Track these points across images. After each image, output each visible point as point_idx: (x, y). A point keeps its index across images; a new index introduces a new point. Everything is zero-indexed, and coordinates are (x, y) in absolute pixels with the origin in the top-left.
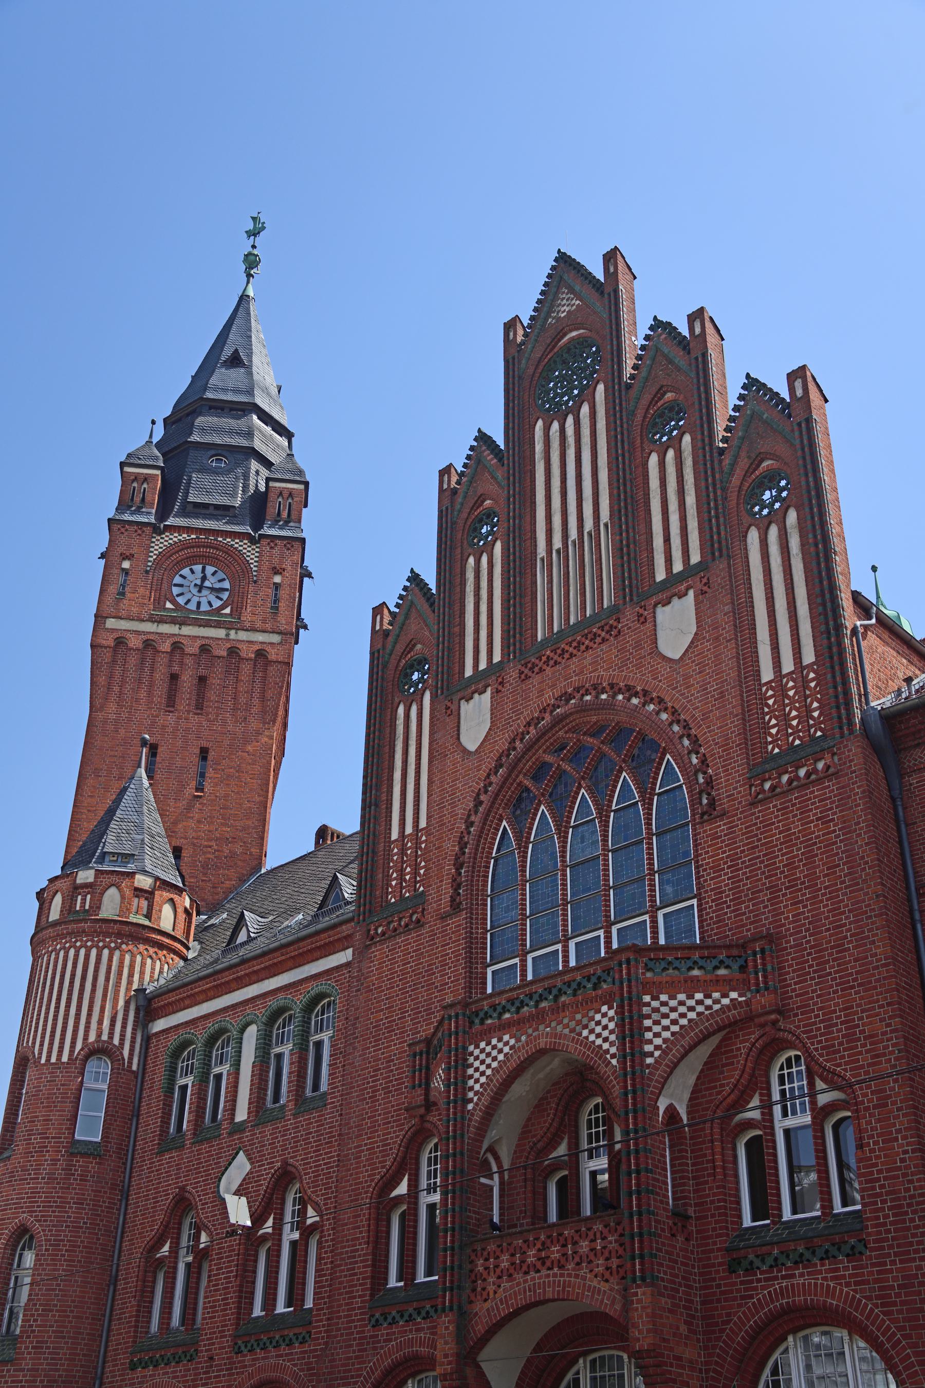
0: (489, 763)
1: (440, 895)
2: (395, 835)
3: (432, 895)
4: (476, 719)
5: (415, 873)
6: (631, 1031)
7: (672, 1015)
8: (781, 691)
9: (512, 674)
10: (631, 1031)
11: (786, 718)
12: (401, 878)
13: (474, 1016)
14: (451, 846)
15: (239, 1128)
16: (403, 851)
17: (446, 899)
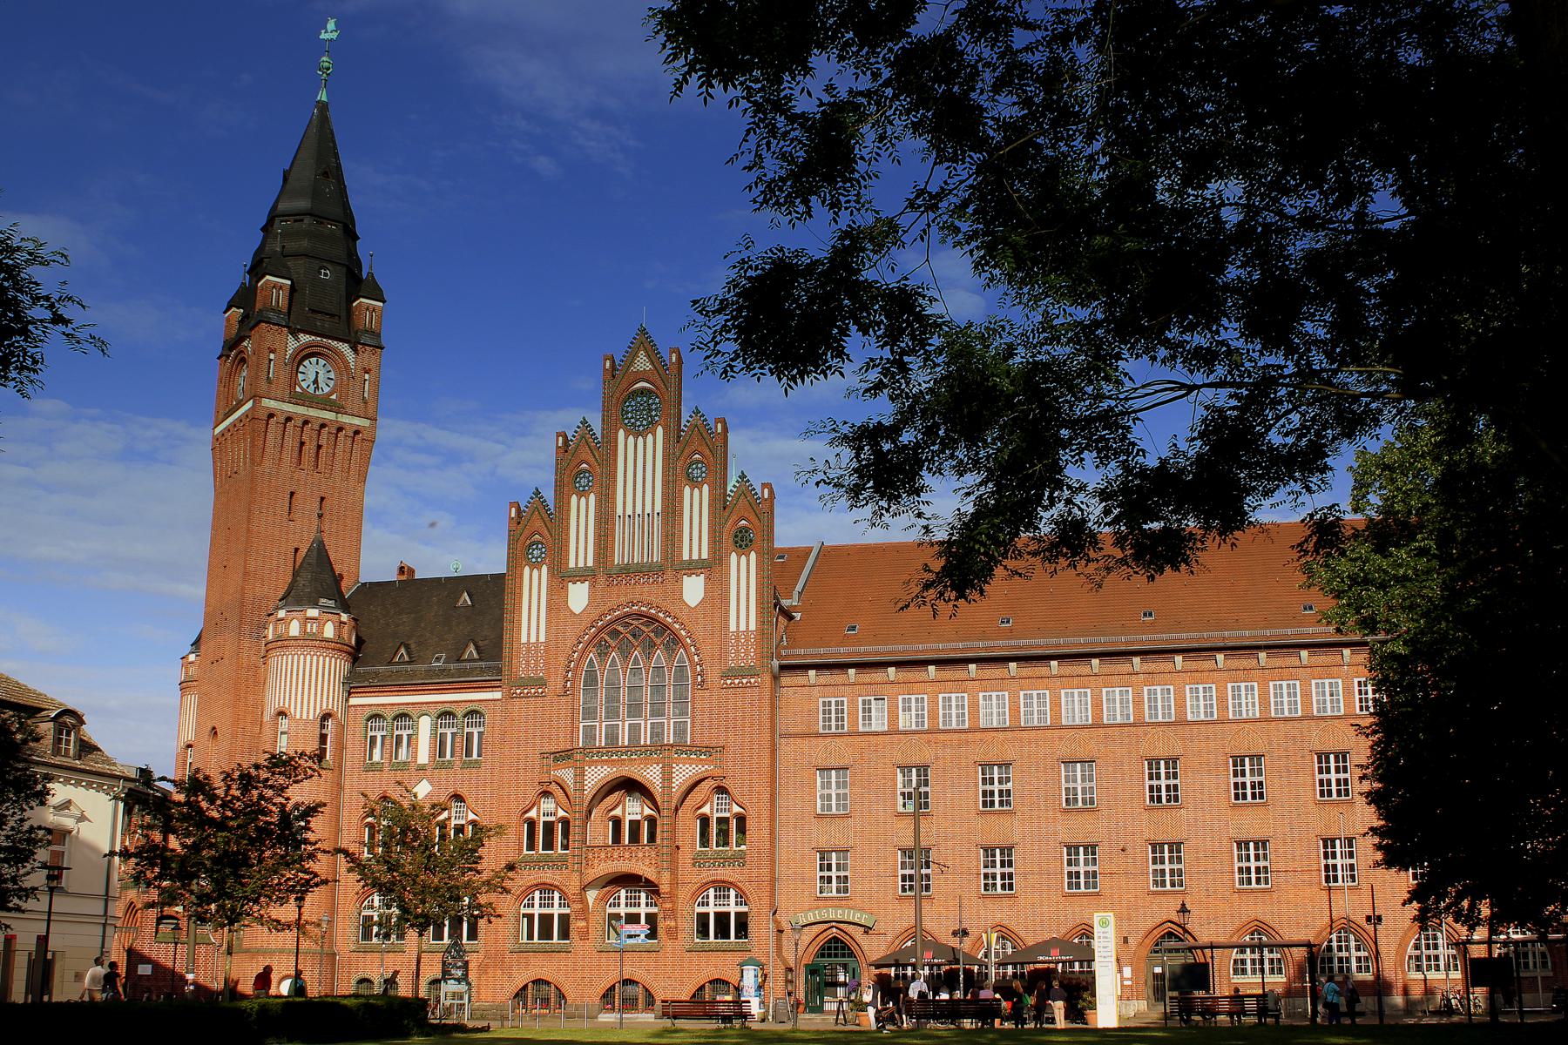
0: (586, 623)
1: (556, 683)
2: (524, 639)
3: (551, 683)
4: (578, 596)
5: (536, 665)
6: (667, 777)
7: (684, 773)
8: (737, 638)
9: (602, 581)
10: (667, 777)
11: (737, 651)
12: (528, 664)
13: (590, 752)
14: (562, 660)
15: (422, 768)
16: (528, 650)
17: (560, 686)
